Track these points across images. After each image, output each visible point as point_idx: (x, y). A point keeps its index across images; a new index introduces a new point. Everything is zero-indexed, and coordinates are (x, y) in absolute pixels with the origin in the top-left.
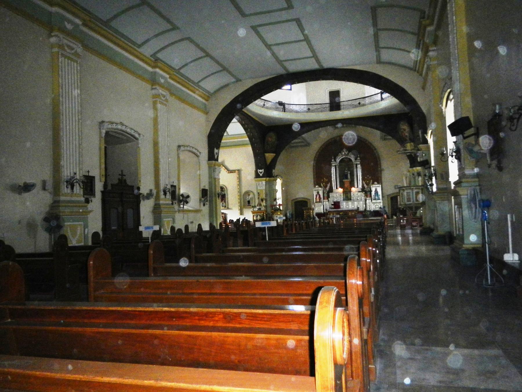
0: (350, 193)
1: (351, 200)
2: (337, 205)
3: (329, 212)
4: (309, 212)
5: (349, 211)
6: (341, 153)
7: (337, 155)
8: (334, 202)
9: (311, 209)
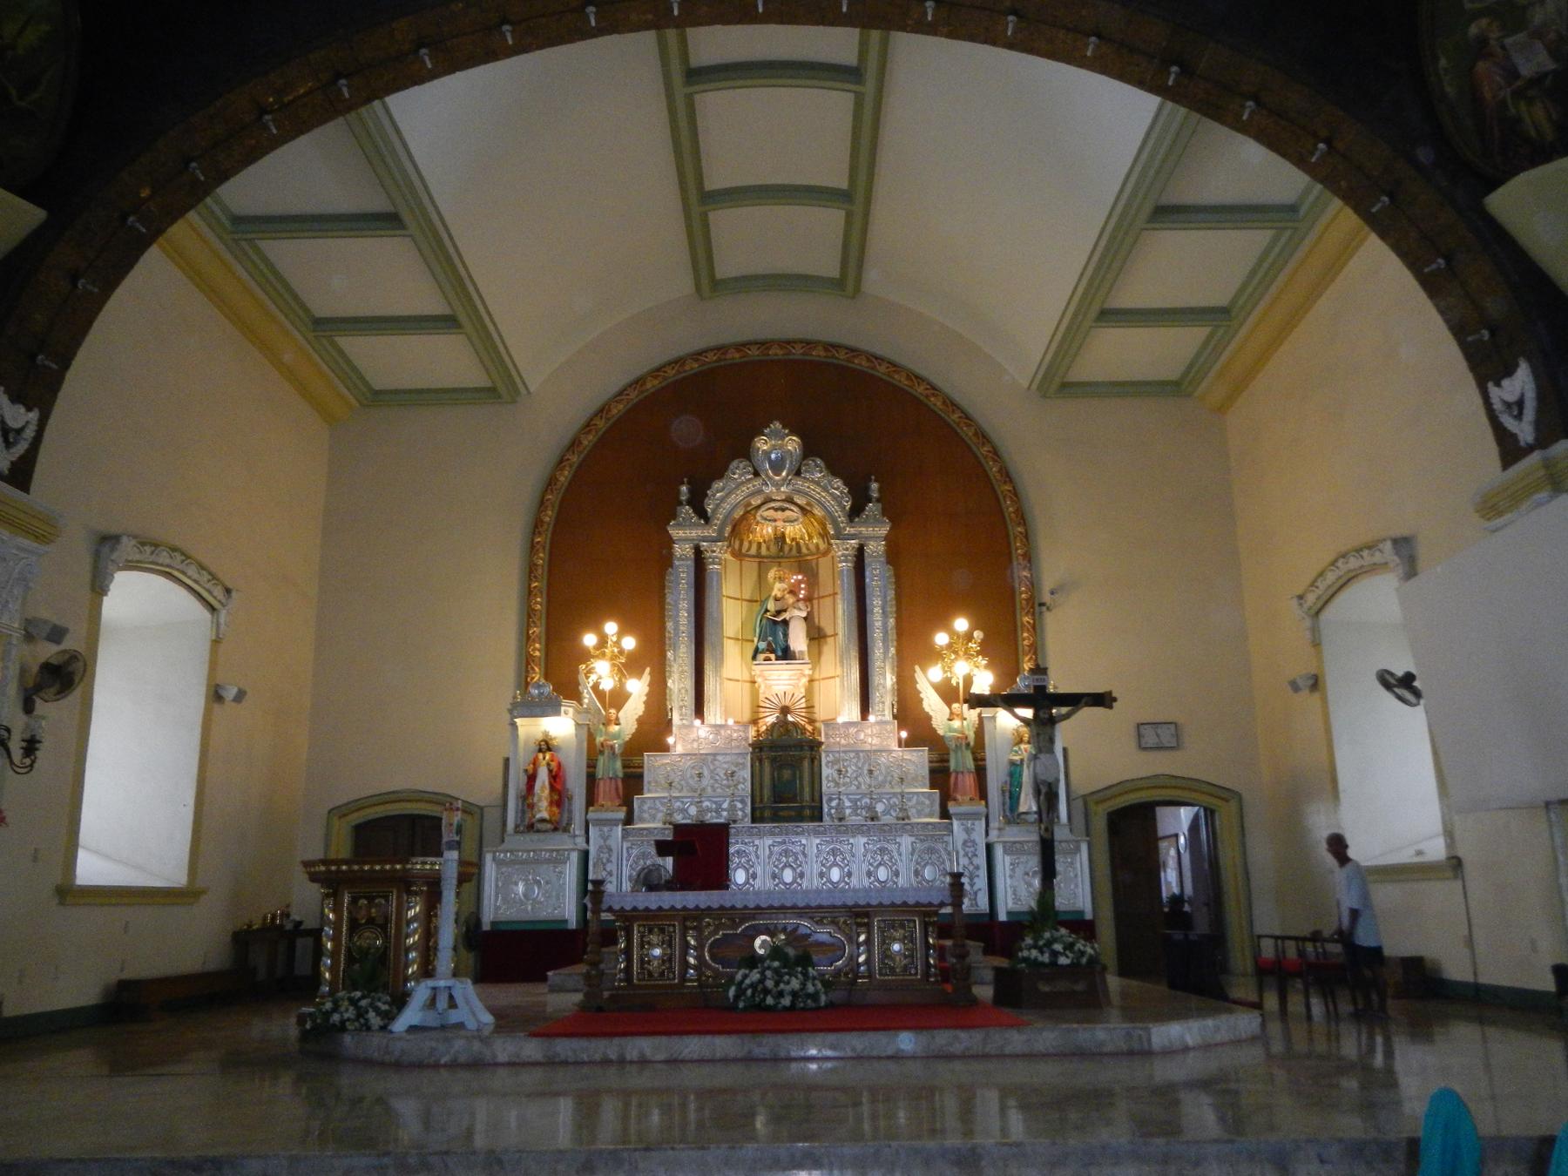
0: (815, 760)
1: (817, 816)
2: (699, 851)
3: (629, 917)
5: (858, 915)
7: (720, 474)
8: (679, 829)
9: (405, 883)
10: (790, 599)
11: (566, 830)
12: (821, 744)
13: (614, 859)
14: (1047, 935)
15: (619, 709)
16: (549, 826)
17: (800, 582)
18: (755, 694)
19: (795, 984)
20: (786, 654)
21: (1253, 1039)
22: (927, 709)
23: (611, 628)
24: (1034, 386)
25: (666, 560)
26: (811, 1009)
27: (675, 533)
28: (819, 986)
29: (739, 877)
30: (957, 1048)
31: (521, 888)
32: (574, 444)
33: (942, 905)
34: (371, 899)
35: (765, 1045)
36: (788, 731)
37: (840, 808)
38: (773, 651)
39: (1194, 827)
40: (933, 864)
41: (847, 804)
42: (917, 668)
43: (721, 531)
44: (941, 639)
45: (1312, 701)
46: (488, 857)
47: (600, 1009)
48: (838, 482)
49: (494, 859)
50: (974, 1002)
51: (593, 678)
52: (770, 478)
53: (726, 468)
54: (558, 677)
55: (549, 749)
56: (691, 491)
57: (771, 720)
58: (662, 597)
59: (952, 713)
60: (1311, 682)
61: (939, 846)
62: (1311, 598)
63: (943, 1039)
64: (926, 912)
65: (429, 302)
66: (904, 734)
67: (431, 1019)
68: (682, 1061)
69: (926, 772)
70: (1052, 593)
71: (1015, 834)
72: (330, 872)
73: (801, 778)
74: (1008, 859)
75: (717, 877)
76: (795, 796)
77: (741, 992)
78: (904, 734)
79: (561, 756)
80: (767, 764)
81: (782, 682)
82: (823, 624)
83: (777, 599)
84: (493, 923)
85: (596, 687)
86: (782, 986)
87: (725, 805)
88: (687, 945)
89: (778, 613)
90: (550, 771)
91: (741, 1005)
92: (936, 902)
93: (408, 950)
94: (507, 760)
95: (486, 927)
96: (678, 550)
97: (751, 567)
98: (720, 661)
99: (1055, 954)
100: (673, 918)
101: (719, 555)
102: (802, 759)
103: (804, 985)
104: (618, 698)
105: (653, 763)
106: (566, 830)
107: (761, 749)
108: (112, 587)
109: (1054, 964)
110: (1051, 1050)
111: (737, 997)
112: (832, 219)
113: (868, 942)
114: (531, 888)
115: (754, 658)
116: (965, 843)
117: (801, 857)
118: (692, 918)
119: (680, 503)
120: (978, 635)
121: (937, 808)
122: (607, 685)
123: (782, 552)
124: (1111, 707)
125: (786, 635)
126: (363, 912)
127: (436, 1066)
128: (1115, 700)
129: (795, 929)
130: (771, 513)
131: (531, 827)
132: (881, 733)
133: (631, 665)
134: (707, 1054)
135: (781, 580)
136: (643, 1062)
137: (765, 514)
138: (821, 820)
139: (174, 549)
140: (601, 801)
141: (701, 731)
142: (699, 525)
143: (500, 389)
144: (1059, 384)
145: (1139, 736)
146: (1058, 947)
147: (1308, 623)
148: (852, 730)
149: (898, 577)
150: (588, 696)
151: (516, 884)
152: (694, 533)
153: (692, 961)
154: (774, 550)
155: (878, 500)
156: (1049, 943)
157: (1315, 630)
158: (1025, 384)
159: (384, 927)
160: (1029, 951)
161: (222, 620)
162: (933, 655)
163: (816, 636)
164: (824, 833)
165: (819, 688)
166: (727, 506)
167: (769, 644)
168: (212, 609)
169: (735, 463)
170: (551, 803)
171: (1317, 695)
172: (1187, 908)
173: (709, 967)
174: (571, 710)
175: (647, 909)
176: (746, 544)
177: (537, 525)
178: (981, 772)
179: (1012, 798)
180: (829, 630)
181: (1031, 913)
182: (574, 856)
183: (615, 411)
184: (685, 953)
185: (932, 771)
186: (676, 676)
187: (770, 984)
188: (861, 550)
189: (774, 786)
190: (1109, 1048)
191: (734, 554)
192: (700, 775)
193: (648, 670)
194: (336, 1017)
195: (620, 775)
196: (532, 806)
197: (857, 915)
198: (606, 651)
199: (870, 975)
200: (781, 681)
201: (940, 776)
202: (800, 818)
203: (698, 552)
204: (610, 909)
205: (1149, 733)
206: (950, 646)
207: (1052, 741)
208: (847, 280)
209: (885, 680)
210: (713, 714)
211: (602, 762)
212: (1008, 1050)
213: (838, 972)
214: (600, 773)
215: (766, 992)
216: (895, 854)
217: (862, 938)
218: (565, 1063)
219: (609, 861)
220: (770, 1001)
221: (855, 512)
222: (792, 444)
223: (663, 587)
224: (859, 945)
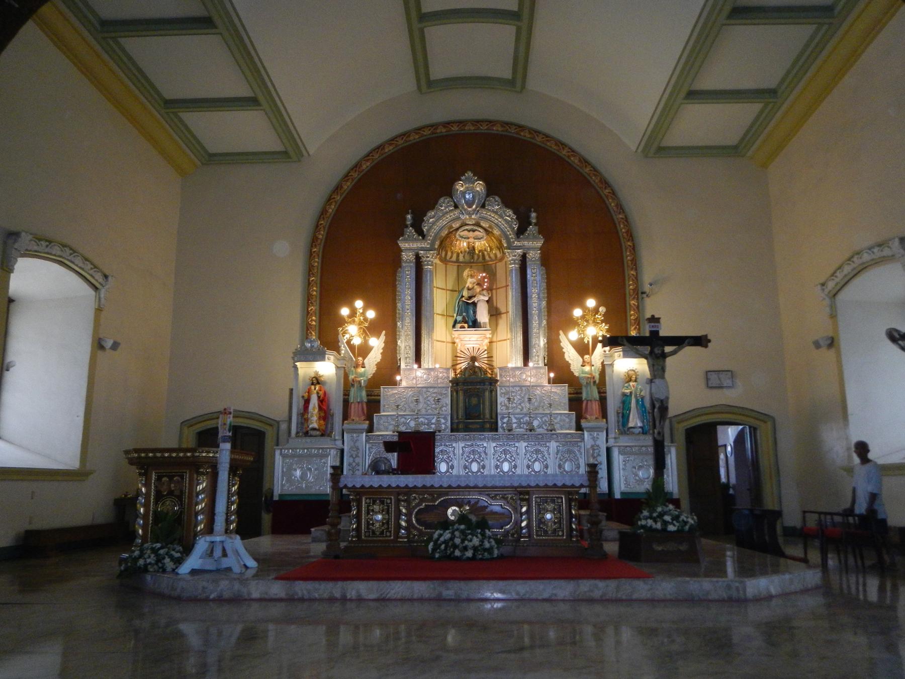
0: (493, 392)
1: (494, 428)
2: (415, 450)
3: (360, 492)
4: (184, 498)
5: (521, 493)
6: (448, 192)
7: (432, 206)
8: (401, 434)
10: (478, 289)
11: (329, 435)
12: (497, 381)
13: (360, 455)
14: (659, 509)
15: (364, 359)
16: (318, 433)
17: (484, 278)
18: (454, 350)
19: (476, 541)
20: (475, 324)
21: (817, 588)
22: (567, 359)
23: (359, 304)
24: (639, 151)
25: (396, 262)
26: (487, 560)
27: (403, 245)
28: (493, 543)
29: (443, 467)
30: (597, 594)
31: (298, 473)
32: (338, 188)
33: (582, 486)
34: (171, 478)
35: (452, 589)
36: (475, 372)
37: (509, 423)
38: (466, 322)
39: (739, 440)
40: (571, 460)
41: (514, 420)
42: (561, 332)
43: (433, 244)
44: (577, 312)
45: (831, 353)
46: (278, 453)
47: (337, 557)
48: (510, 212)
49: (281, 454)
50: (605, 556)
51: (347, 336)
52: (465, 210)
53: (436, 202)
54: (326, 338)
55: (318, 383)
56: (413, 218)
57: (463, 366)
58: (394, 287)
59: (584, 361)
60: (829, 342)
61: (576, 449)
62: (831, 285)
63: (585, 586)
64: (569, 491)
65: (243, 91)
66: (552, 375)
67: (210, 565)
68: (389, 600)
69: (566, 401)
70: (651, 285)
71: (625, 441)
72: (139, 457)
73: (484, 404)
74: (621, 457)
75: (428, 467)
76: (480, 415)
77: (436, 547)
78: (552, 375)
79: (327, 388)
80: (461, 393)
81: (471, 341)
82: (499, 306)
83: (469, 289)
84: (280, 495)
85: (349, 342)
86: (466, 542)
87: (434, 421)
88: (399, 513)
89: (470, 298)
90: (319, 397)
91: (437, 555)
92: (577, 485)
93: (197, 514)
94: (291, 390)
95: (276, 498)
96: (405, 256)
97: (452, 269)
98: (431, 329)
99: (665, 523)
100: (391, 493)
101: (432, 261)
102: (484, 391)
103: (482, 541)
104: (364, 351)
105: (386, 393)
106: (329, 435)
107: (457, 384)
108: (16, 267)
109: (664, 530)
110: (668, 597)
111: (434, 550)
112: (506, 33)
113: (527, 512)
114: (295, 473)
115: (454, 326)
116: (592, 446)
117: (483, 455)
118: (408, 491)
119: (407, 227)
120: (602, 309)
121: (574, 424)
122: (357, 341)
123: (473, 259)
124: (706, 346)
125: (475, 312)
126: (165, 487)
127: (207, 600)
128: (709, 341)
129: (477, 503)
130: (466, 233)
131: (306, 434)
132: (537, 375)
133: (372, 329)
134: (407, 594)
135: (472, 276)
136: (360, 600)
137: (462, 234)
138: (496, 430)
139: (64, 246)
140: (352, 417)
141: (419, 373)
142: (419, 240)
143: (290, 152)
144: (656, 148)
145: (707, 379)
146: (667, 518)
147: (827, 301)
148: (518, 373)
149: (548, 274)
150: (344, 349)
151: (295, 470)
152: (415, 245)
153: (403, 524)
154: (467, 258)
155: (536, 224)
156: (661, 515)
157: (833, 308)
158: (634, 148)
159: (180, 498)
160: (646, 521)
161: (102, 296)
162: (572, 323)
163: (495, 313)
164: (498, 439)
165: (498, 346)
166: (436, 228)
167: (464, 318)
168: (96, 288)
169: (442, 200)
170: (320, 418)
171: (833, 351)
172: (731, 492)
173: (415, 528)
174: (332, 357)
175: (371, 487)
176: (449, 254)
177: (314, 241)
178: (603, 400)
179: (624, 417)
180: (503, 310)
181: (647, 492)
182: (333, 452)
183: (364, 167)
184: (398, 518)
185: (570, 400)
186: (403, 338)
187: (457, 541)
188: (524, 257)
189: (466, 408)
190: (714, 596)
191: (441, 260)
192: (417, 401)
193: (384, 332)
194: (141, 562)
195: (365, 400)
196: (307, 420)
197: (521, 493)
198: (356, 319)
199: (530, 535)
200: (471, 341)
201: (576, 403)
202: (482, 429)
203: (418, 258)
204: (345, 487)
205: (713, 377)
206: (583, 317)
207: (663, 370)
208: (516, 81)
209: (540, 342)
210: (427, 362)
211: (353, 392)
212: (635, 596)
213: (507, 533)
214: (351, 400)
215: (455, 547)
216: (545, 453)
217: (524, 509)
218: (302, 600)
219: (357, 456)
220: (457, 553)
221: (521, 232)
222: (480, 186)
223: (395, 280)
224: (522, 514)
